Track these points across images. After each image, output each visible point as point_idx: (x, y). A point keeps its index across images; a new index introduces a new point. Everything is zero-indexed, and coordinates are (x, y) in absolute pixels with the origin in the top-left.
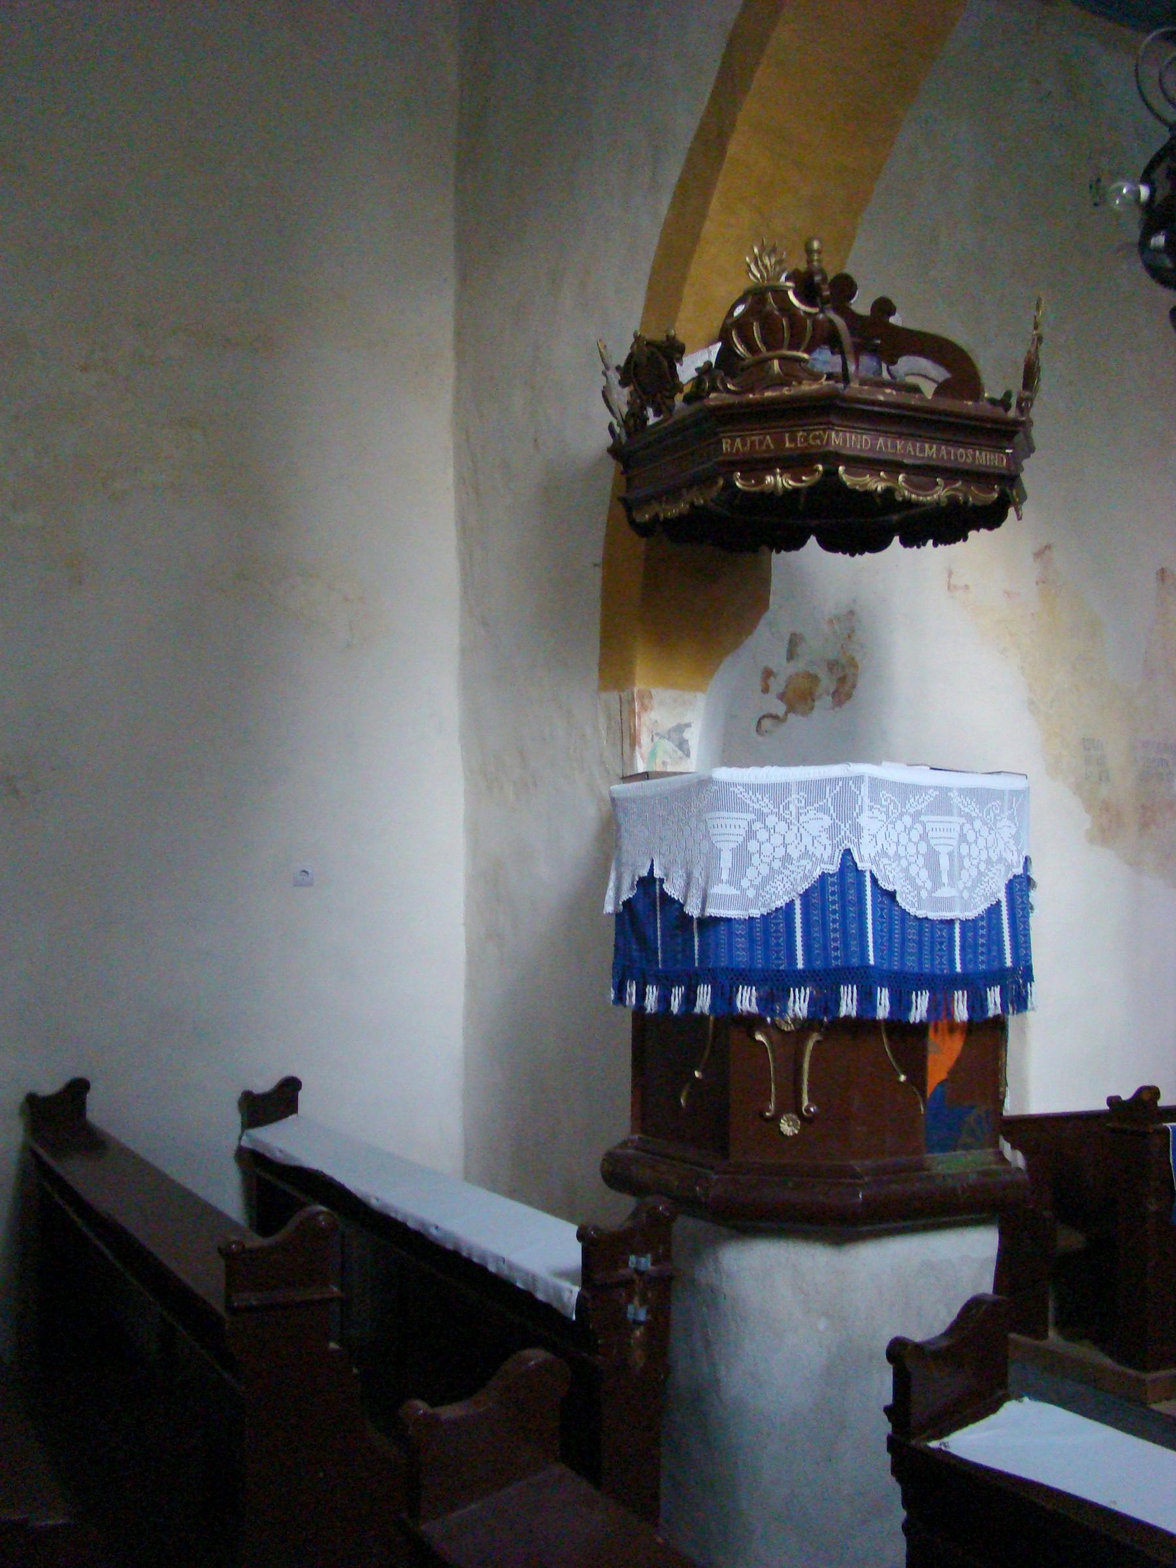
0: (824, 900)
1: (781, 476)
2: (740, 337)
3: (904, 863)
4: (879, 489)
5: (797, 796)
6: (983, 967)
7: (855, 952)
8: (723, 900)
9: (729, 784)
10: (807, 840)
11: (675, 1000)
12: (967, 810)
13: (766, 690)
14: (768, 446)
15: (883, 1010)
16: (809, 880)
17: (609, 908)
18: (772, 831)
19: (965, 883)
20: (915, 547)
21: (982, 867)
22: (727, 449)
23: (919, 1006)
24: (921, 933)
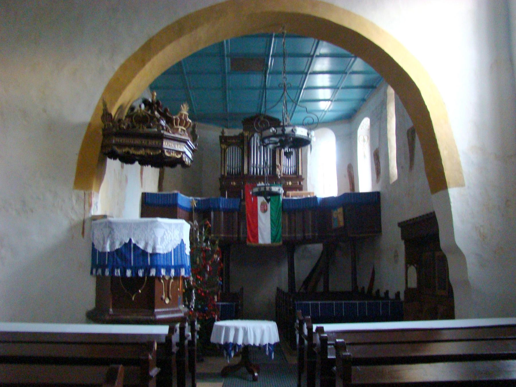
8: (160, 249)
10: (175, 236)
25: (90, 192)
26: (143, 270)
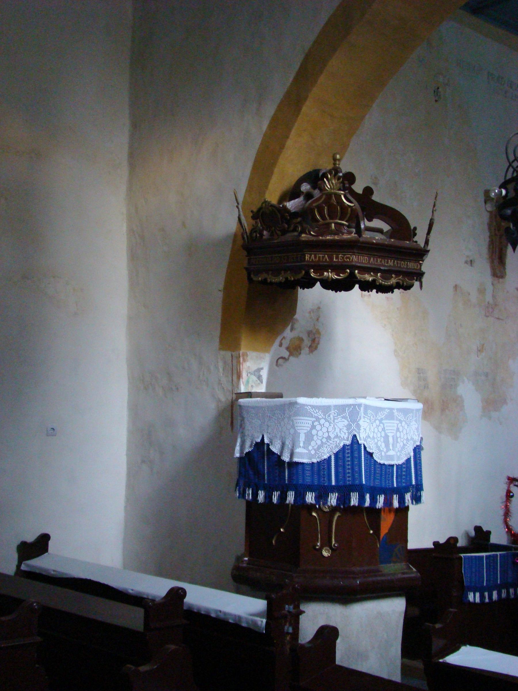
0: (344, 457)
1: (331, 273)
2: (318, 211)
3: (376, 440)
4: (370, 279)
5: (334, 411)
6: (404, 485)
7: (358, 478)
8: (301, 455)
9: (304, 405)
10: (337, 430)
11: (274, 497)
12: (400, 418)
14: (326, 259)
15: (367, 503)
16: (338, 447)
17: (237, 455)
18: (323, 426)
19: (398, 449)
20: (367, 292)
21: (405, 442)
22: (307, 259)
23: (380, 502)
24: (381, 470)
25: (237, 354)
26: (279, 492)
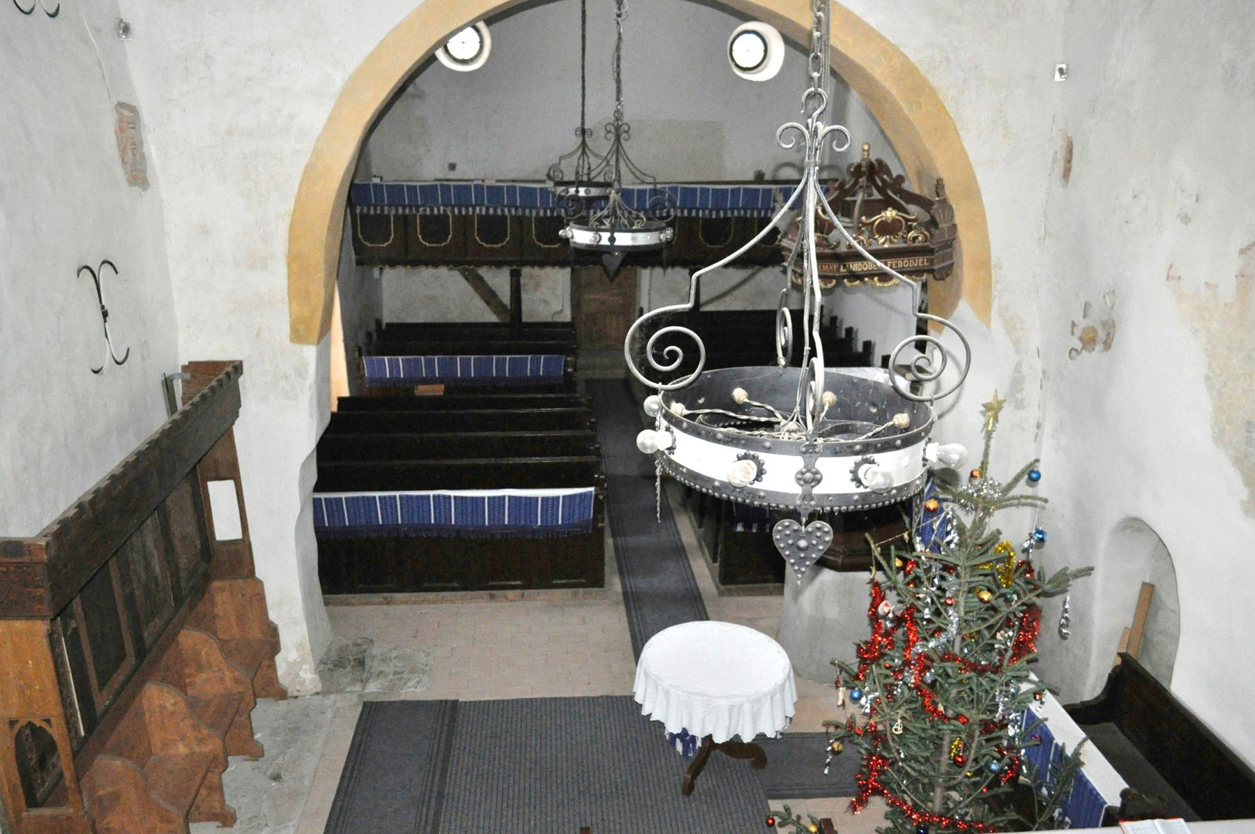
13: (1073, 333)
